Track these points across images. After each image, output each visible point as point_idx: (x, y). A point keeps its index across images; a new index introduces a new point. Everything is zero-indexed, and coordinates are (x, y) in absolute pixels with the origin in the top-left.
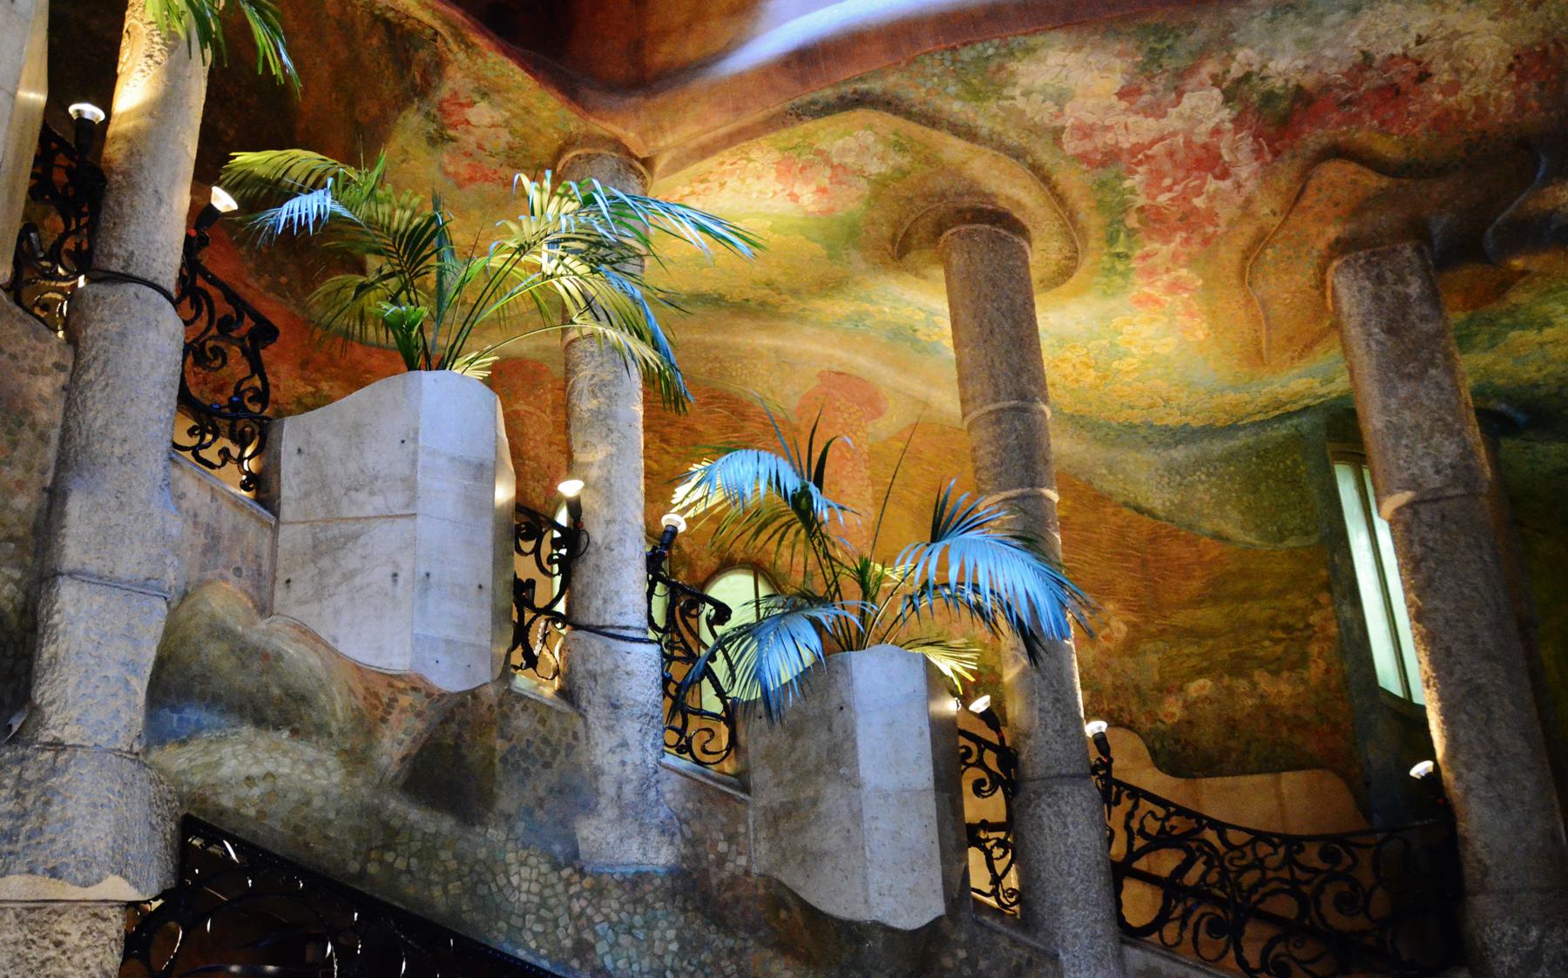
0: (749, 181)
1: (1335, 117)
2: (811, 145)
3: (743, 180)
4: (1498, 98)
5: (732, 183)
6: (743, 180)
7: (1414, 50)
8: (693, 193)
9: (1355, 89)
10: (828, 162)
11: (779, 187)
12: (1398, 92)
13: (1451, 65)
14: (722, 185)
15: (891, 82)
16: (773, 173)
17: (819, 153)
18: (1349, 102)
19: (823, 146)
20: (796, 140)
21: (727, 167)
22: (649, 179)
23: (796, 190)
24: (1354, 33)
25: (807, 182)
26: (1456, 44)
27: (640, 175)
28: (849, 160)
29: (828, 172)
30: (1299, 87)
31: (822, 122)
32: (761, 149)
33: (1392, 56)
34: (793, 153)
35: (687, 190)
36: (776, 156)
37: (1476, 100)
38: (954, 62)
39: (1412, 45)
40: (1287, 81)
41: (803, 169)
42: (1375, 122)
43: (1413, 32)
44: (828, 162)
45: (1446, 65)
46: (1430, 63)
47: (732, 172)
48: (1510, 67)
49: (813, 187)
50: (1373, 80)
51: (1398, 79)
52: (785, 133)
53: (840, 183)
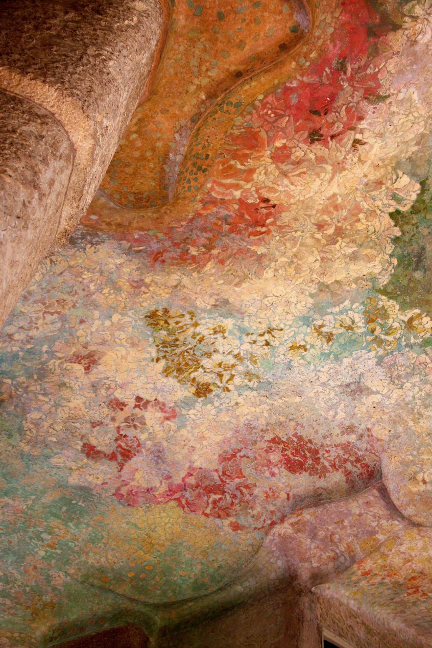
1: (334, 51)
4: (237, 187)
7: (351, 136)
9: (351, 80)
12: (316, 113)
13: (309, 160)
18: (342, 68)
24: (415, 96)
26: (329, 168)
30: (396, 27)
33: (360, 118)
37: (251, 171)
39: (359, 136)
40: (415, 18)
42: (295, 84)
43: (371, 141)
45: (312, 156)
46: (326, 144)
48: (267, 201)
50: (348, 95)
51: (330, 117)
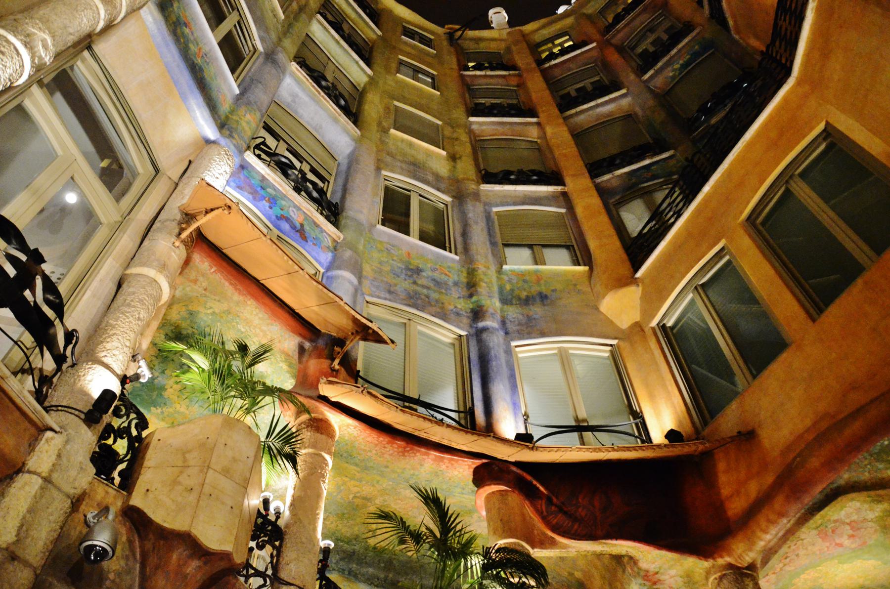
0: (810, 548)
2: (829, 520)
3: (806, 549)
5: (802, 552)
6: (806, 549)
8: (785, 565)
10: (844, 523)
11: (828, 544)
14: (797, 555)
15: (845, 476)
16: (820, 540)
17: (836, 521)
19: (835, 517)
20: (820, 522)
21: (793, 547)
22: (755, 574)
23: (838, 541)
25: (841, 536)
27: (747, 576)
28: (855, 517)
29: (848, 527)
31: (827, 509)
32: (803, 532)
34: (822, 527)
35: (781, 565)
36: (815, 532)
38: (871, 456)
41: (833, 531)
44: (844, 523)
47: (798, 548)
49: (846, 537)
52: (811, 521)
53: (859, 529)
